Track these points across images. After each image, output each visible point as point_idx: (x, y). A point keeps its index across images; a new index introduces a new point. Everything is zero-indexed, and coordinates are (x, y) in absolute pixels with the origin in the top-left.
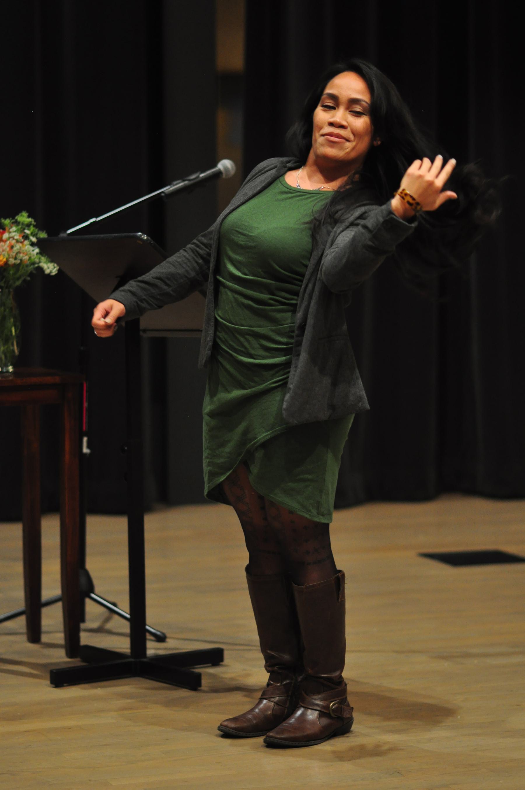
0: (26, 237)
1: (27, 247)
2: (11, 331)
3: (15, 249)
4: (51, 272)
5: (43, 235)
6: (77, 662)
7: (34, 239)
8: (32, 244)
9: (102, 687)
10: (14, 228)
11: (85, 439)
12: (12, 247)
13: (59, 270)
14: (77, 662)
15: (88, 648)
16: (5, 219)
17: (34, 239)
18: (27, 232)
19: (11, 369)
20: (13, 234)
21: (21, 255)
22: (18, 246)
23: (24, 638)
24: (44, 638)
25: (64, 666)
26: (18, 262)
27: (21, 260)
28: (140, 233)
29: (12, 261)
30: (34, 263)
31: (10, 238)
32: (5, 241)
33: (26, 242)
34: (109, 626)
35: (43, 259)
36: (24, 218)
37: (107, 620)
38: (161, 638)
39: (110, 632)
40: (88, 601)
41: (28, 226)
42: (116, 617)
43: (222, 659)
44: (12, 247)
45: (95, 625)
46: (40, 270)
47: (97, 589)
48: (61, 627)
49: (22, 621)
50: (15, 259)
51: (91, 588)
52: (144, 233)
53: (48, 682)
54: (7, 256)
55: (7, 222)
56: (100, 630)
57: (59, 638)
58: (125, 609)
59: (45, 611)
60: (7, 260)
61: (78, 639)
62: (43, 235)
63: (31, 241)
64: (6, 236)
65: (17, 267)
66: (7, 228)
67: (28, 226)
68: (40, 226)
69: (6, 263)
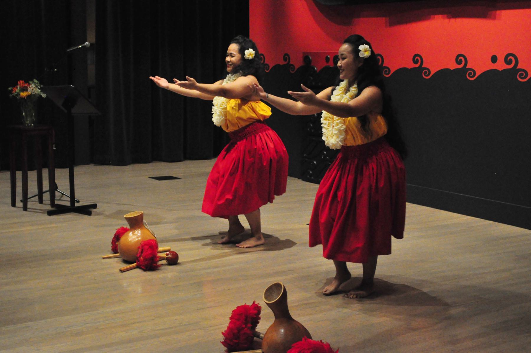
0: (37, 87)
1: (37, 89)
2: (33, 114)
3: (34, 90)
4: (44, 97)
5: (42, 86)
6: (53, 209)
7: (39, 87)
8: (39, 88)
9: (63, 215)
10: (33, 84)
11: (54, 145)
12: (33, 90)
13: (47, 96)
14: (53, 209)
15: (57, 204)
16: (30, 81)
17: (39, 87)
18: (37, 85)
19: (33, 125)
20: (33, 86)
21: (36, 92)
22: (34, 89)
23: (38, 202)
24: (44, 202)
25: (50, 210)
26: (35, 94)
27: (36, 93)
28: (72, 86)
29: (33, 93)
30: (39, 94)
31: (32, 87)
32: (31, 88)
33: (37, 88)
34: (62, 199)
35: (42, 93)
36: (35, 81)
37: (62, 197)
38: (78, 202)
39: (63, 200)
40: (56, 191)
41: (37, 83)
42: (64, 196)
43: (97, 207)
44: (33, 90)
45: (58, 198)
46: (41, 96)
47: (58, 189)
48: (49, 199)
49: (37, 197)
50: (34, 93)
51: (57, 188)
52: (73, 85)
53: (47, 214)
54: (31, 92)
55: (31, 82)
56: (59, 200)
57: (49, 202)
58: (68, 193)
59: (44, 194)
60: (31, 93)
61: (54, 202)
62: (42, 86)
63: (38, 88)
64: (31, 86)
65: (34, 95)
66: (31, 84)
67: (37, 83)
68: (41, 83)
69: (31, 94)
